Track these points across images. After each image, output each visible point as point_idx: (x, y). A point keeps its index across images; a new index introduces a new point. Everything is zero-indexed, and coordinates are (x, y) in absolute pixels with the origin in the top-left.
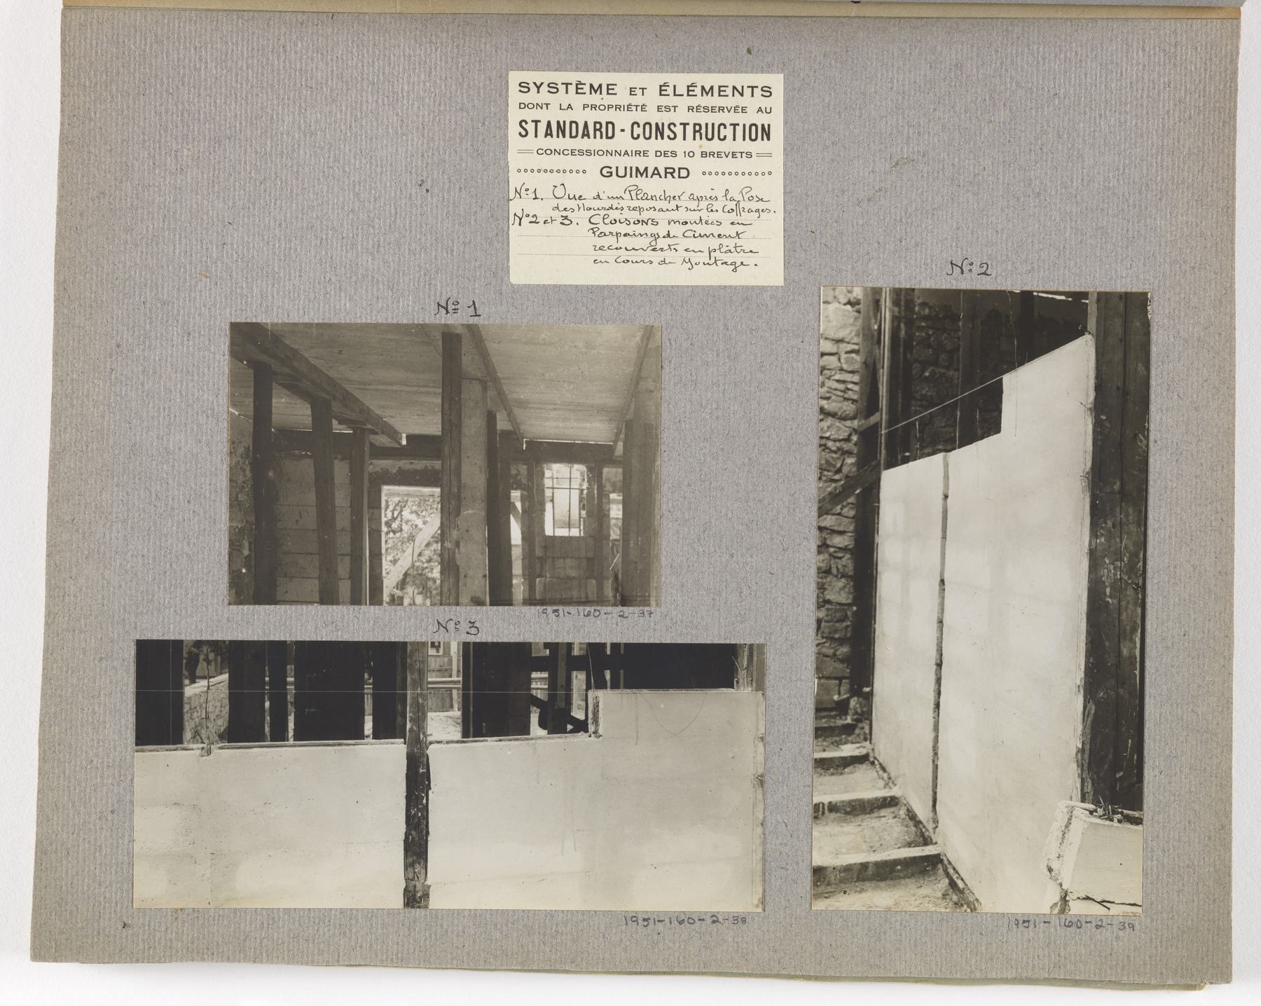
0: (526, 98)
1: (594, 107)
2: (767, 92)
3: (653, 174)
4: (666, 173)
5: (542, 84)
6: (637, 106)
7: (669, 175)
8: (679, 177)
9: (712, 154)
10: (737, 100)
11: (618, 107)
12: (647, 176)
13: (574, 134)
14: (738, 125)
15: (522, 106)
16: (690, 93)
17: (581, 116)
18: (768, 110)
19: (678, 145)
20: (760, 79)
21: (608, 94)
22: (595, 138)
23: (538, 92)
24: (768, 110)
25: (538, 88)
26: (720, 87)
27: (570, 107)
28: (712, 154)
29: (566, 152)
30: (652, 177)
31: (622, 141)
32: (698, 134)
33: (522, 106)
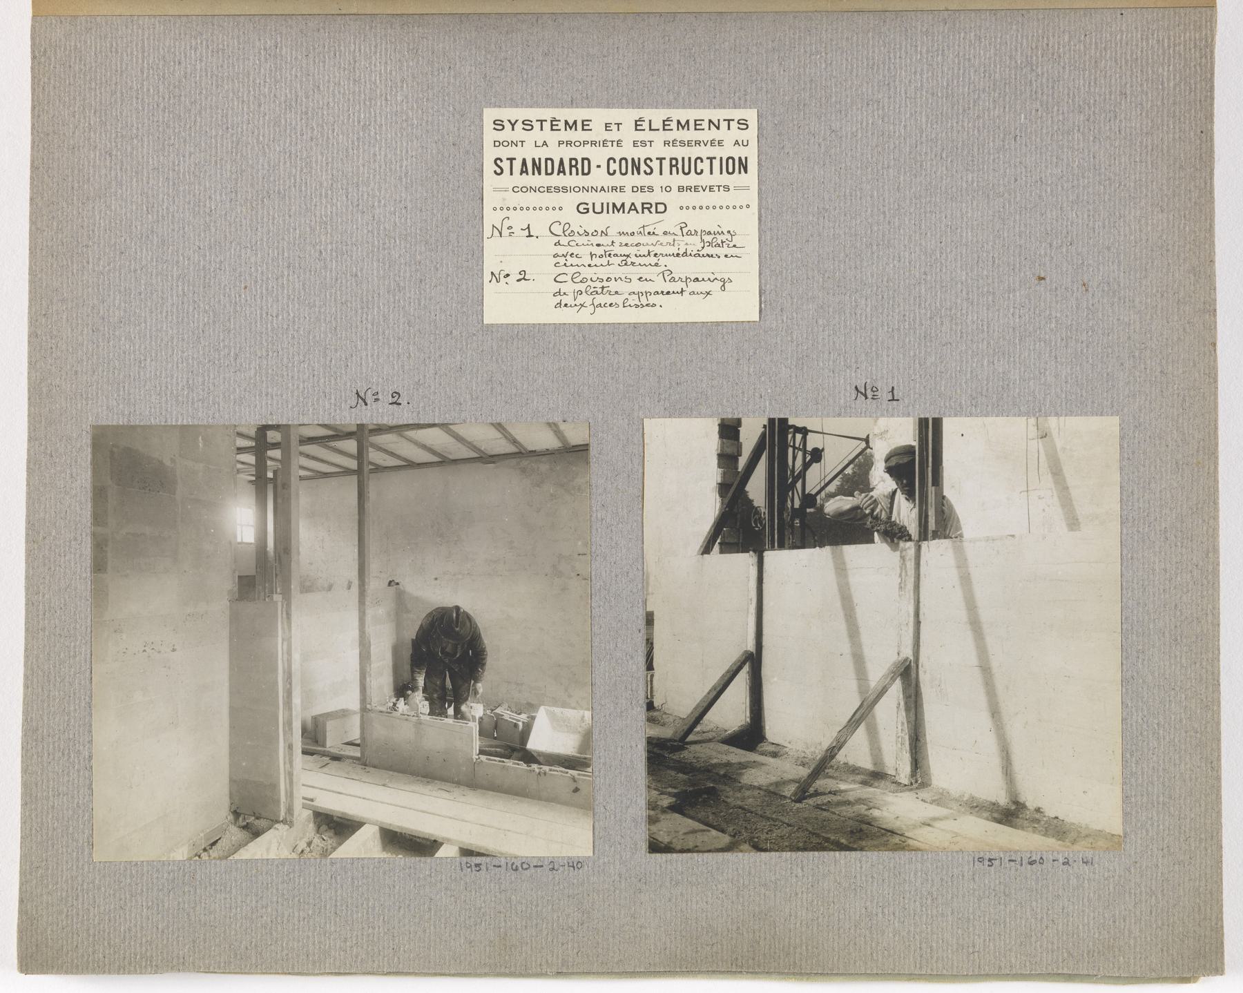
0: (501, 136)
1: (569, 143)
2: (743, 124)
3: (630, 209)
4: (643, 208)
5: (517, 121)
7: (646, 211)
8: (657, 212)
10: (714, 134)
11: (594, 143)
12: (624, 212)
13: (549, 171)
14: (715, 158)
15: (497, 144)
16: (666, 127)
17: (557, 153)
18: (745, 143)
19: (655, 180)
20: (737, 114)
21: (583, 129)
22: (571, 174)
23: (513, 129)
24: (745, 143)
25: (513, 125)
26: (696, 121)
27: (545, 144)
29: (541, 189)
31: (598, 177)
32: (674, 169)
33: (497, 144)
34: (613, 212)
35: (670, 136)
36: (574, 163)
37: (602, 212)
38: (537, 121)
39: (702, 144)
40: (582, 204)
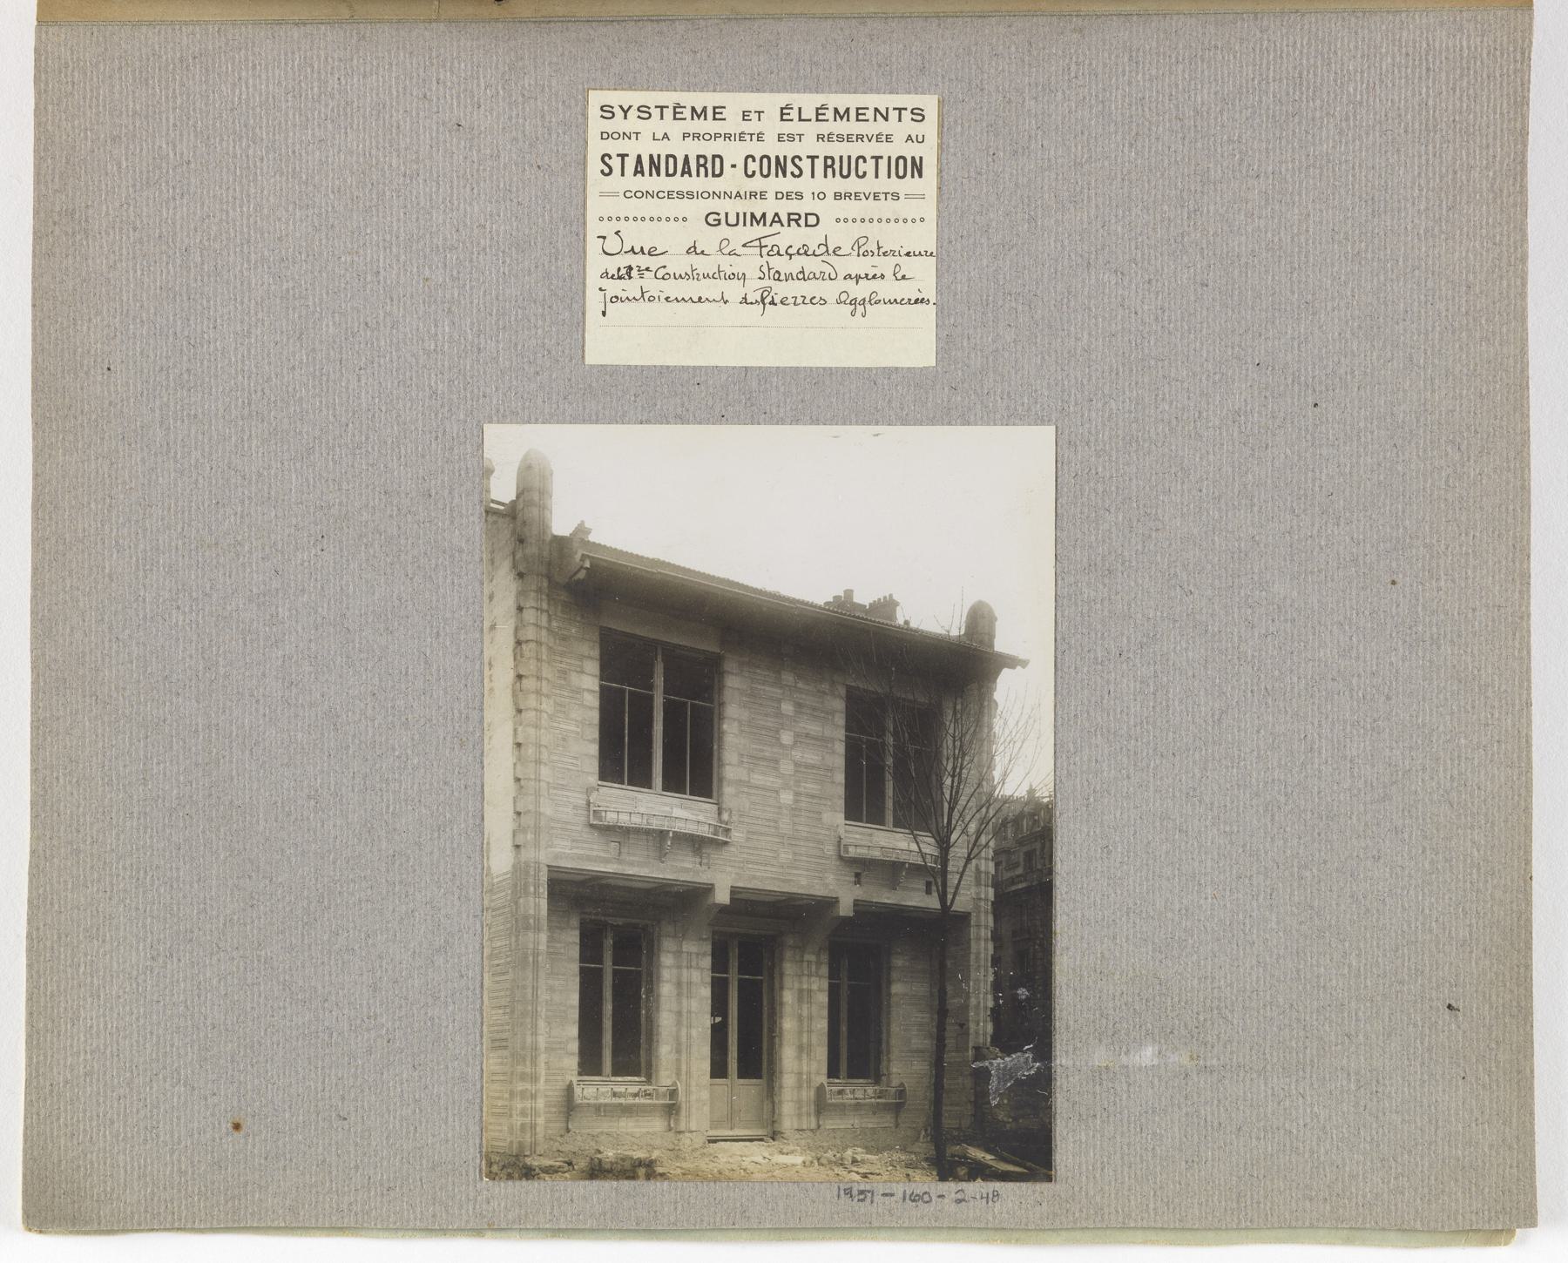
0: (609, 126)
1: (697, 136)
2: (918, 115)
3: (773, 221)
4: (789, 220)
5: (630, 107)
6: (751, 135)
7: (793, 223)
8: (806, 225)
9: (848, 196)
10: (881, 126)
11: (727, 137)
12: (765, 225)
13: (671, 171)
14: (881, 157)
15: (605, 136)
17: (680, 148)
18: (920, 139)
19: (805, 184)
20: (909, 101)
21: (714, 119)
22: (698, 175)
23: (625, 118)
24: (920, 139)
25: (626, 112)
26: (858, 109)
27: (666, 136)
28: (848, 196)
29: (661, 195)
30: (771, 225)
31: (732, 180)
32: (830, 171)
34: (752, 225)
35: (824, 128)
36: (702, 161)
37: (737, 224)
38: (656, 107)
39: (865, 139)
40: (707, 216)
